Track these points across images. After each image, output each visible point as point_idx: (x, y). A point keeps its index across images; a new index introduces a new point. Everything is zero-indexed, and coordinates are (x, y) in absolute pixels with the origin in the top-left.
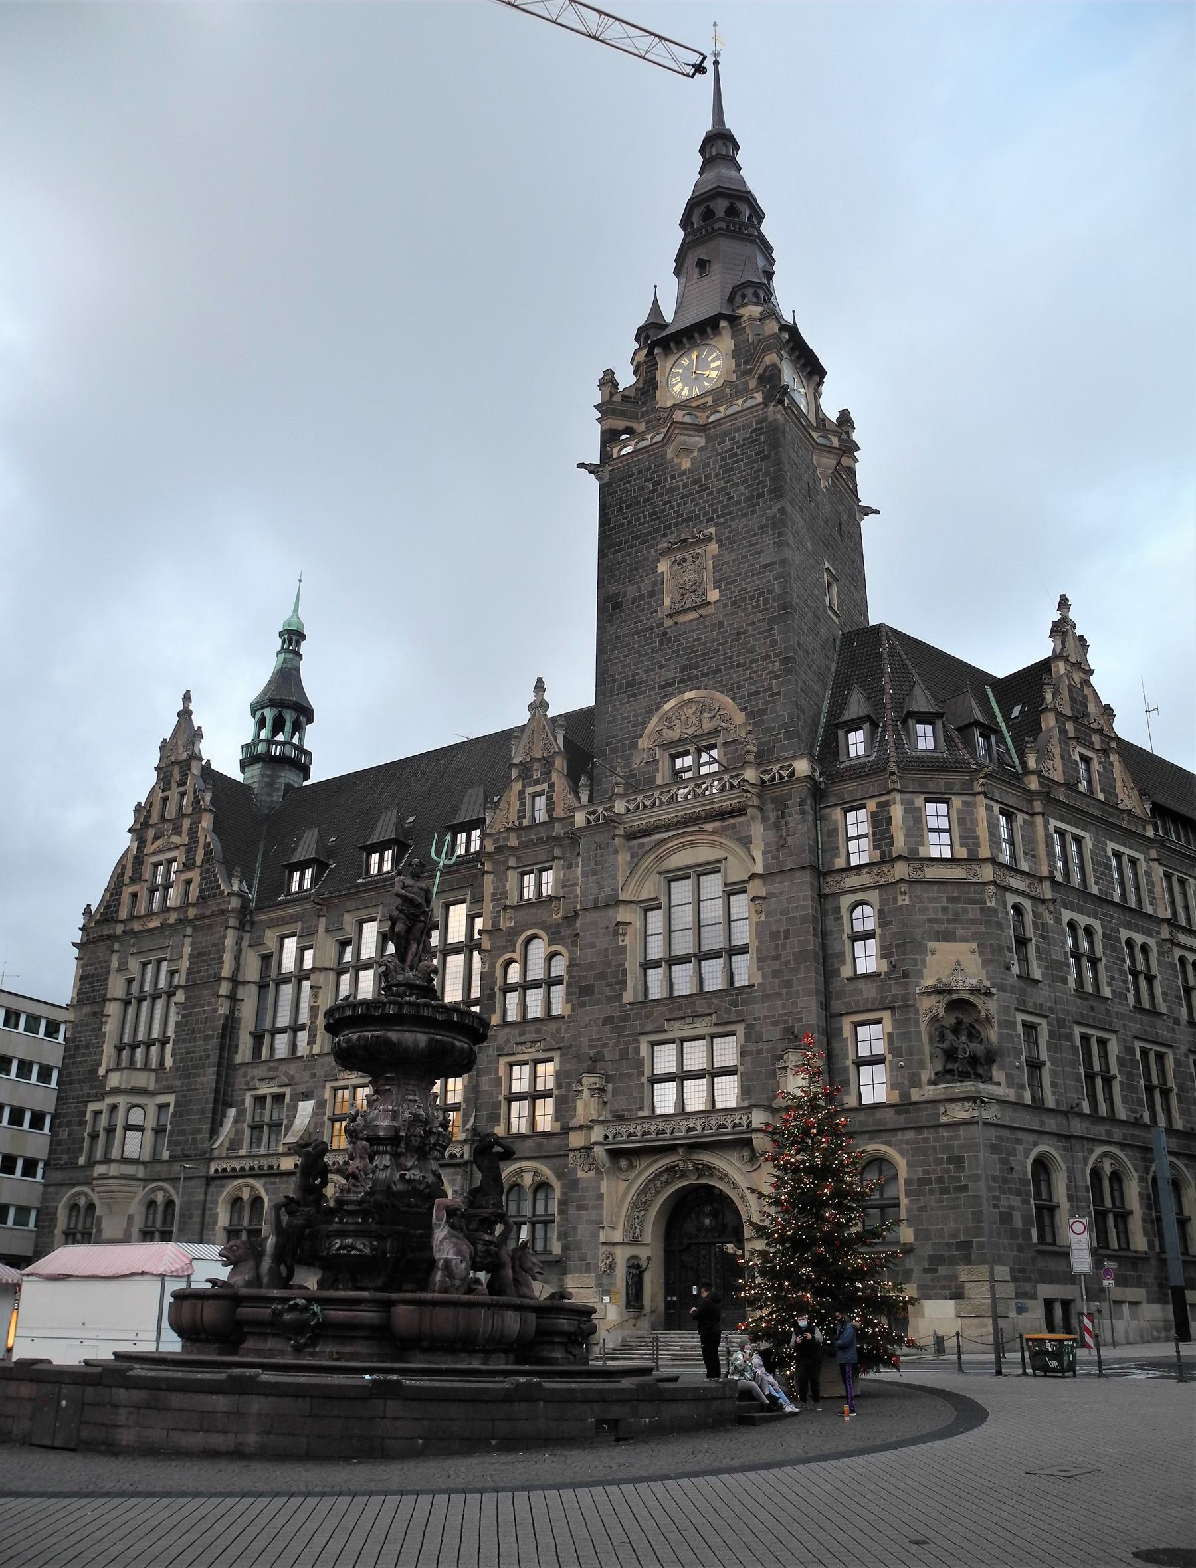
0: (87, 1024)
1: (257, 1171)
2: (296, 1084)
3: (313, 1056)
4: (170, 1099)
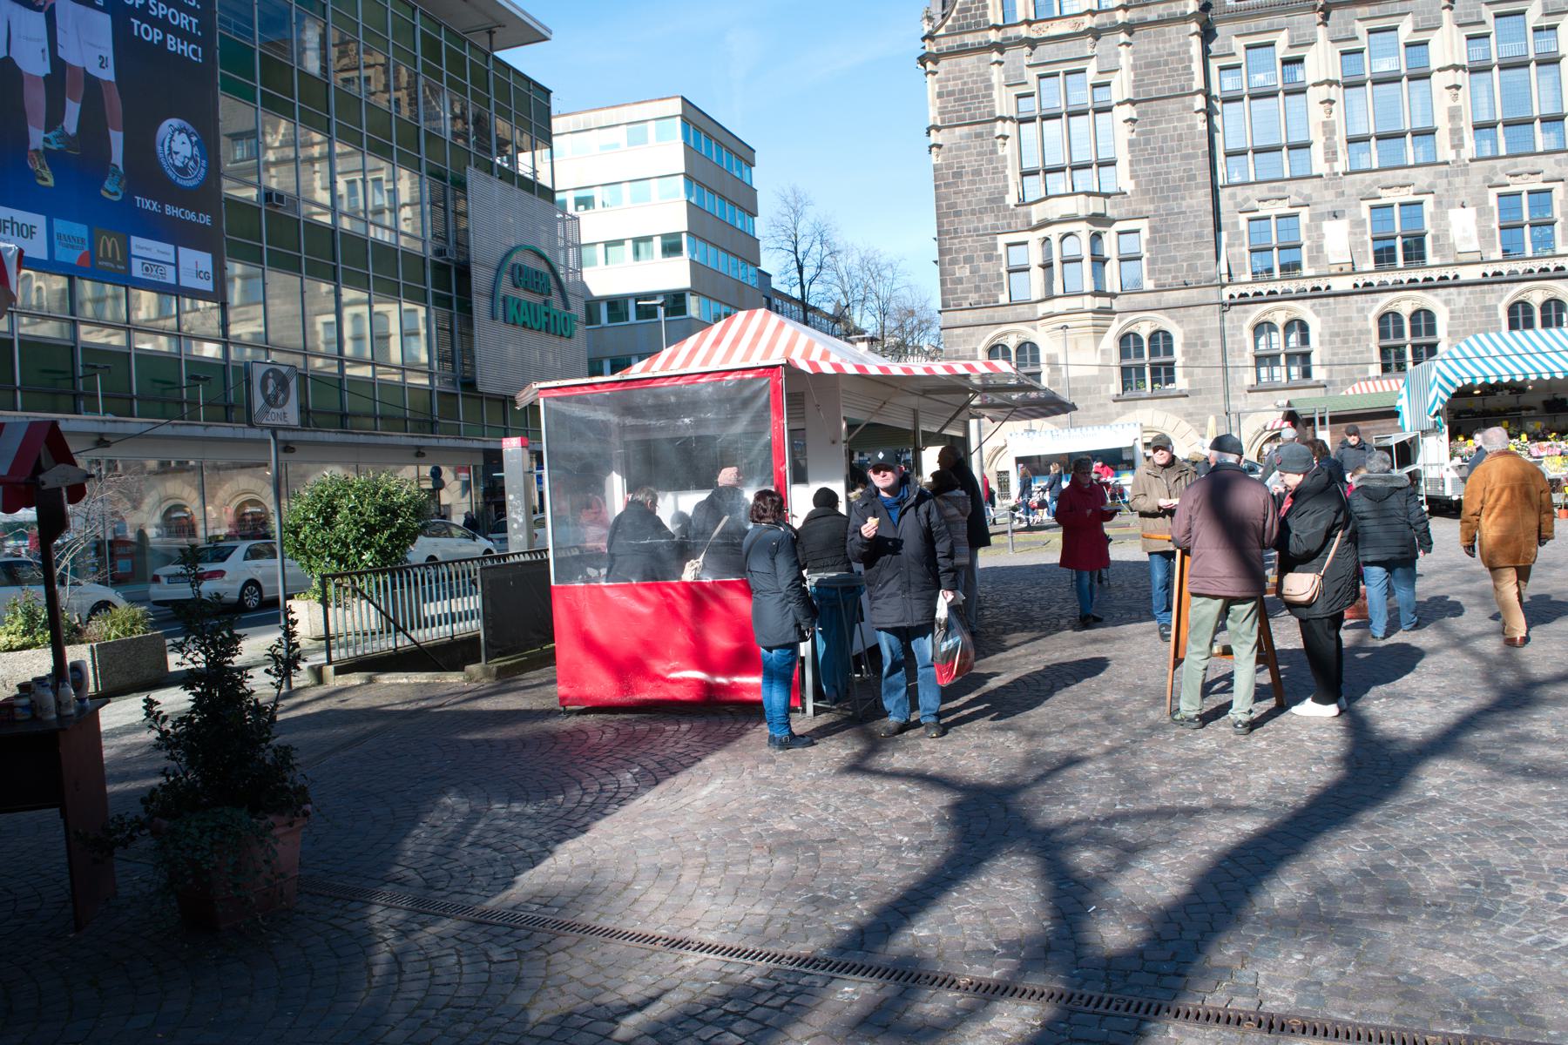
0: (969, 147)
1: (1323, 292)
2: (1316, 203)
3: (1337, 174)
4: (1143, 225)
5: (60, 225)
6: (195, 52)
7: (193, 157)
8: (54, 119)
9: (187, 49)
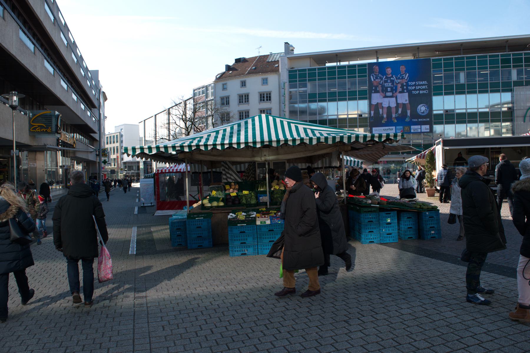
5: (397, 127)
6: (426, 92)
7: (426, 110)
8: (397, 111)
9: (425, 92)
